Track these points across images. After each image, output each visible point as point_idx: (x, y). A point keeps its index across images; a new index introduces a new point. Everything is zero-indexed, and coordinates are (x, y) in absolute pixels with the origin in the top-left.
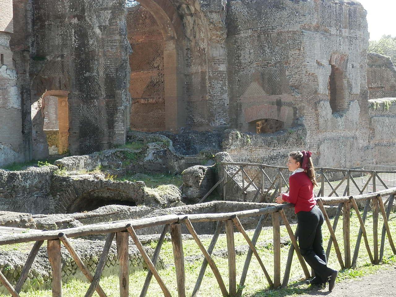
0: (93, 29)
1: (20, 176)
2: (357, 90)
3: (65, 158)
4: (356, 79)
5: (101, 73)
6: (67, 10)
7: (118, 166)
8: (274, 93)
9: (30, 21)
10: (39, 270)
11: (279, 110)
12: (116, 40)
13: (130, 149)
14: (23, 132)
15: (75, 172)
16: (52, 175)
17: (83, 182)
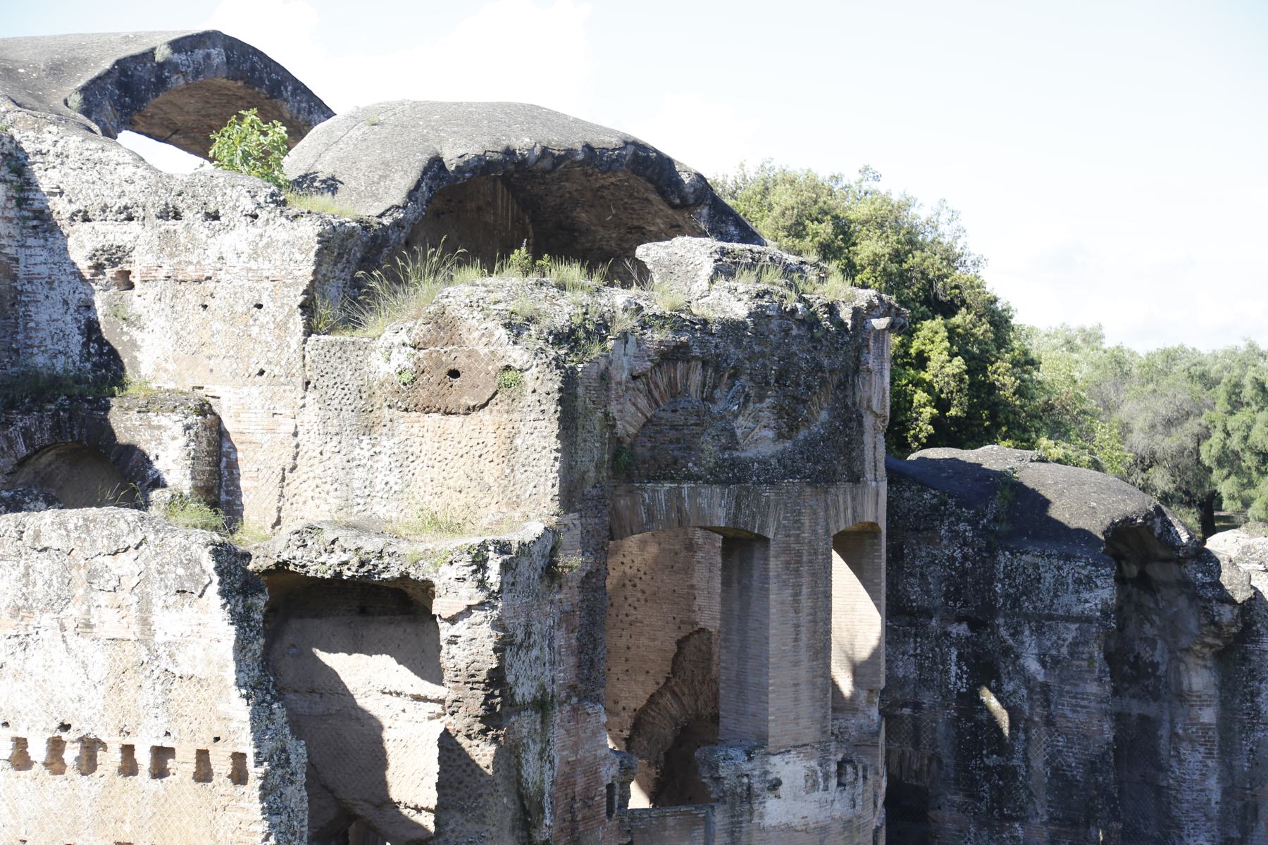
0: (1018, 657)
5: (1038, 763)
12: (1087, 694)
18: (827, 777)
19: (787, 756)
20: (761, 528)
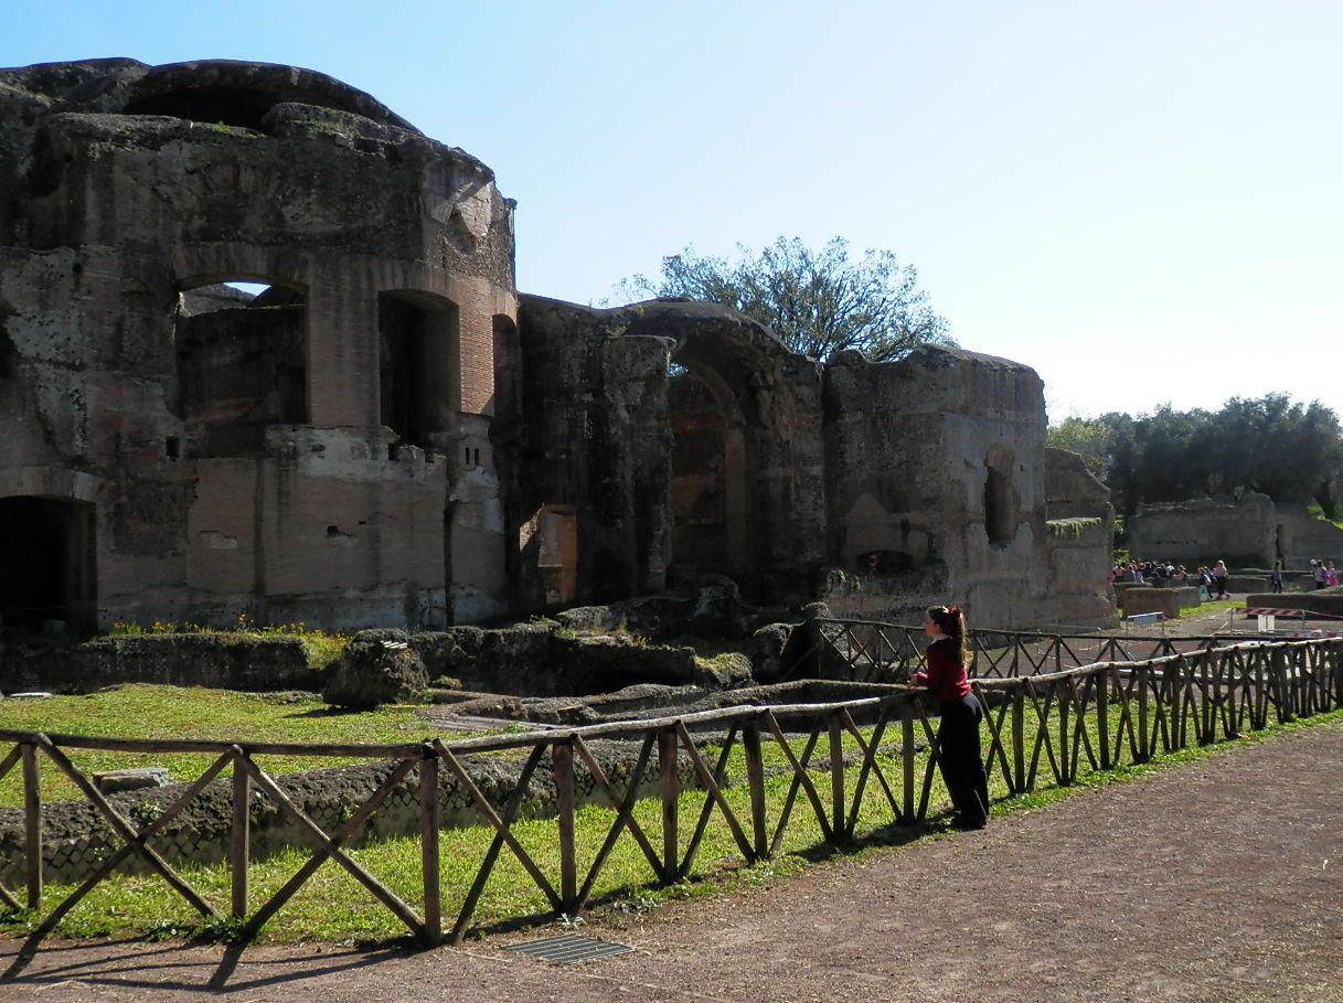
1: (502, 638)
2: (1028, 506)
3: (572, 610)
4: (1027, 489)
5: (629, 479)
6: (578, 381)
7: (653, 623)
8: (897, 509)
9: (519, 398)
10: (535, 789)
11: (905, 537)
13: (671, 596)
14: (507, 569)
15: (587, 632)
16: (550, 636)
17: (602, 646)
18: (375, 452)
19: (331, 432)
20: (301, 277)
